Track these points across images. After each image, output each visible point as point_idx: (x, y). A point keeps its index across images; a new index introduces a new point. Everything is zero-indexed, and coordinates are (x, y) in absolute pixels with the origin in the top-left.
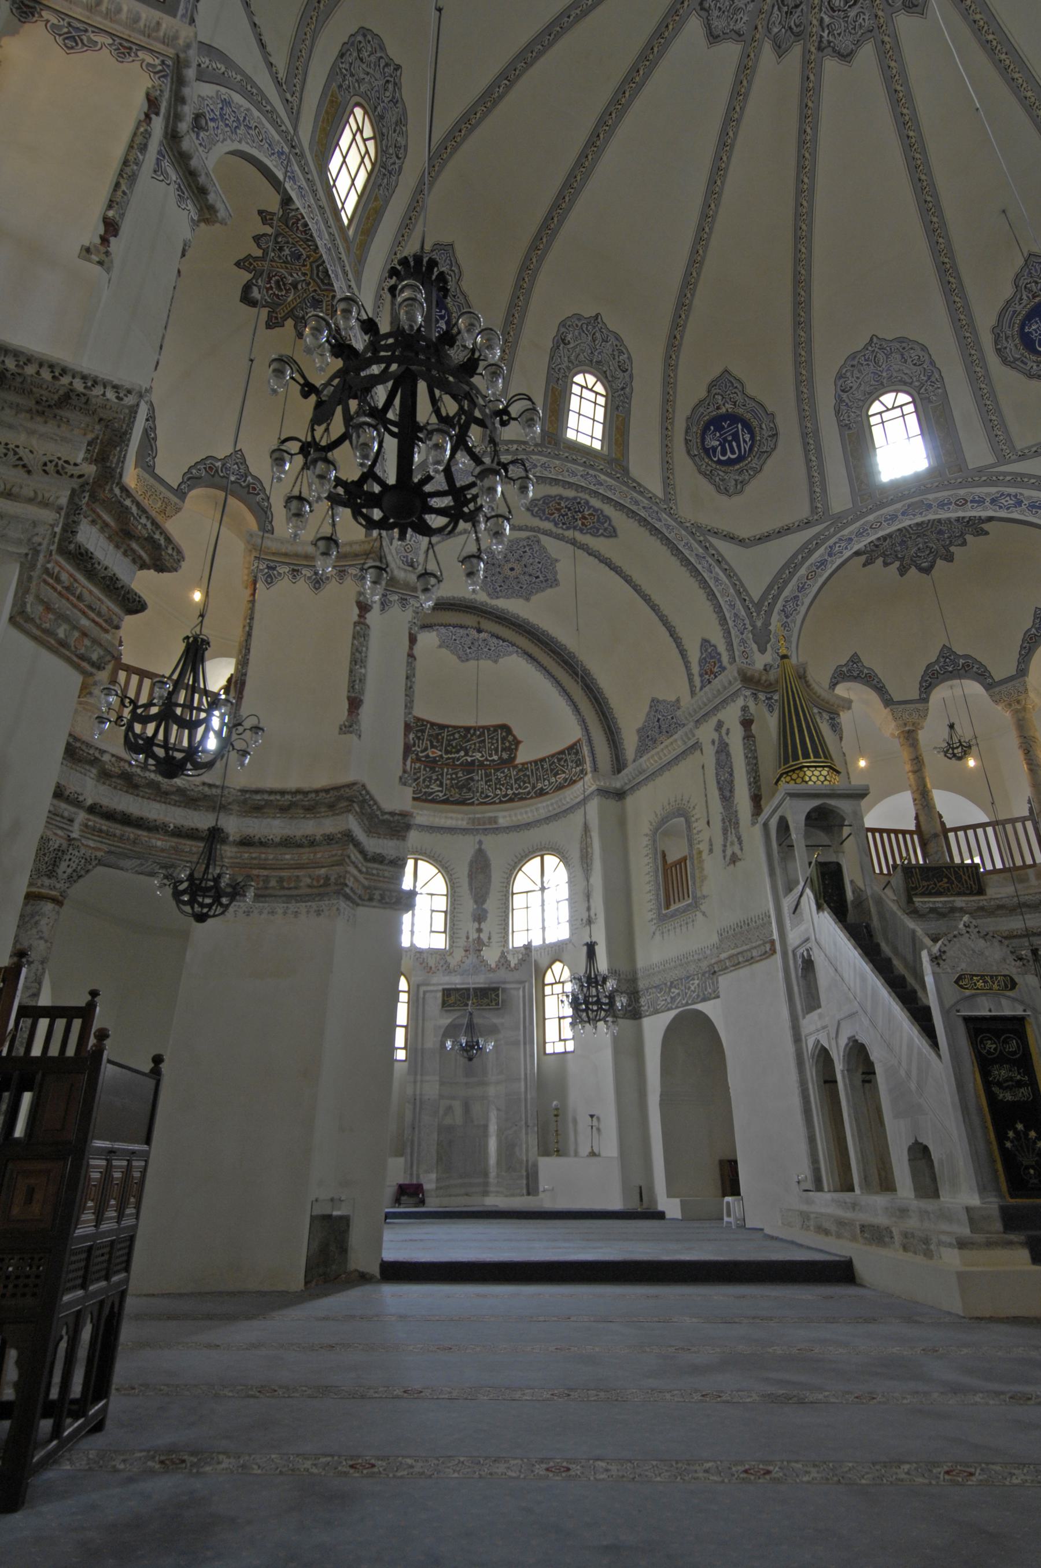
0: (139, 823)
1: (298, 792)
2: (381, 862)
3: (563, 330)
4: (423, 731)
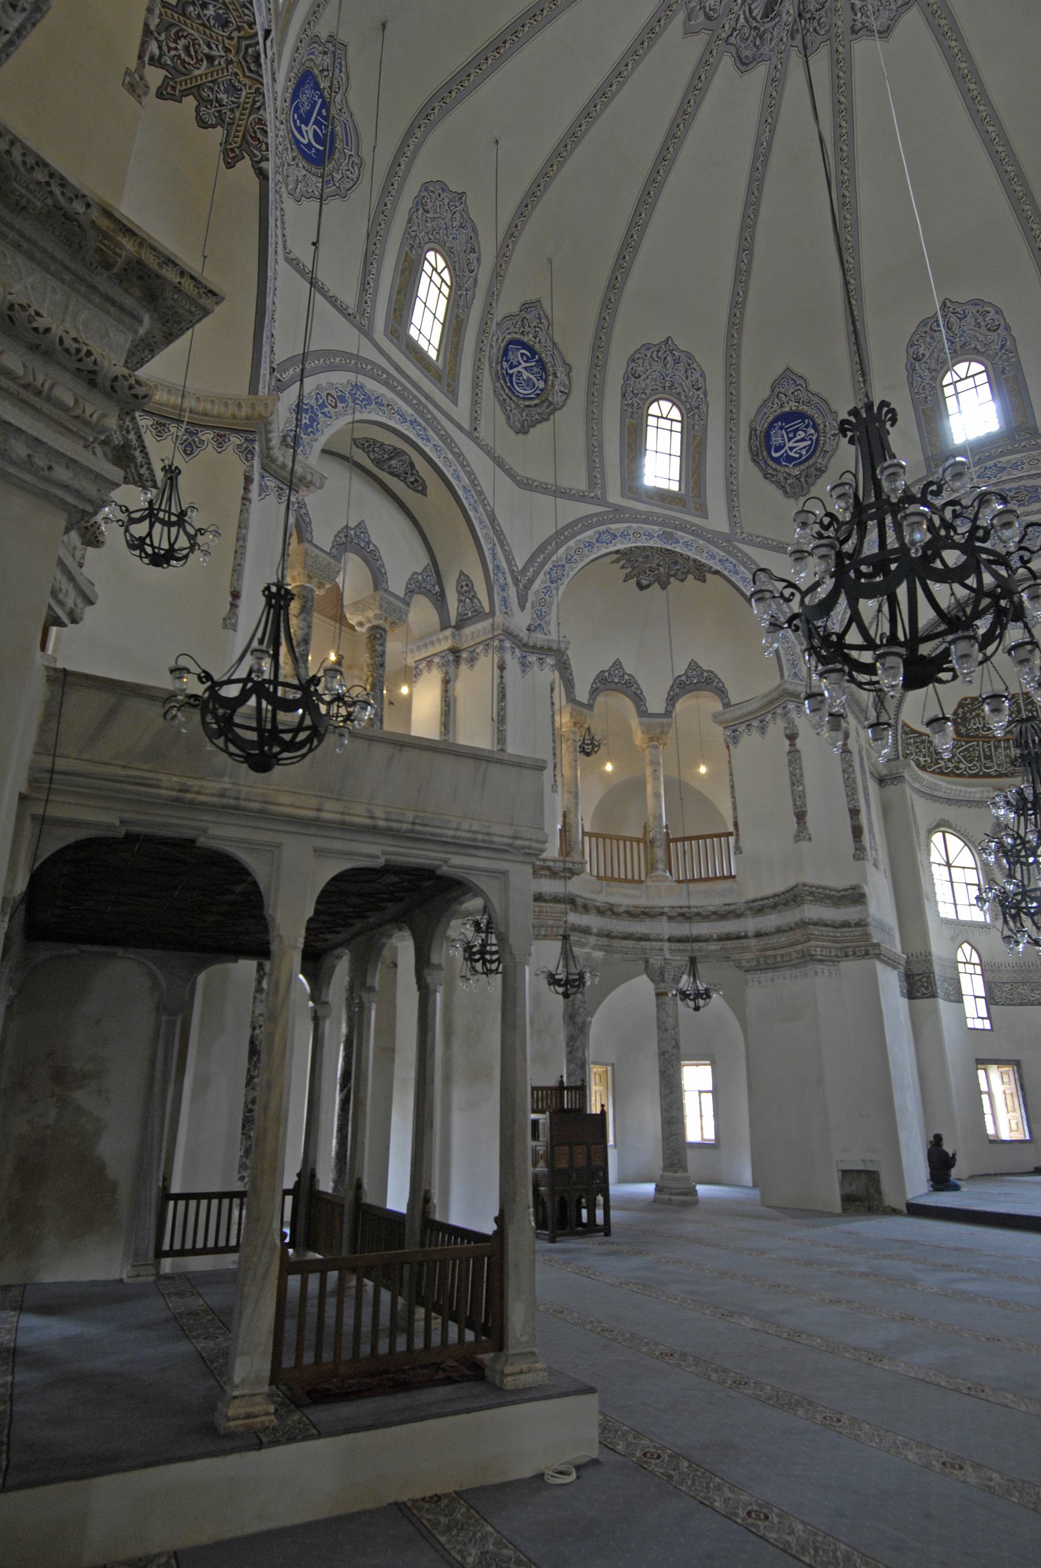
0: (697, 939)
1: (774, 896)
2: (849, 926)
3: (911, 350)
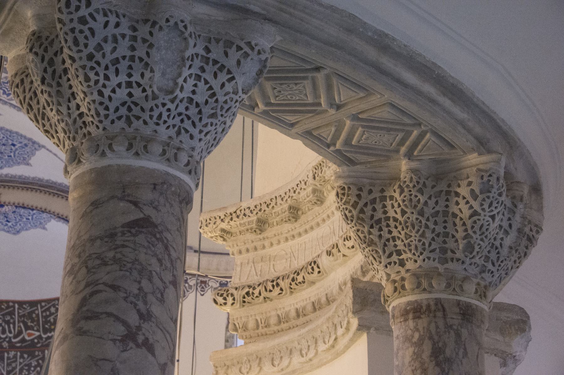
4: (12, 314)
